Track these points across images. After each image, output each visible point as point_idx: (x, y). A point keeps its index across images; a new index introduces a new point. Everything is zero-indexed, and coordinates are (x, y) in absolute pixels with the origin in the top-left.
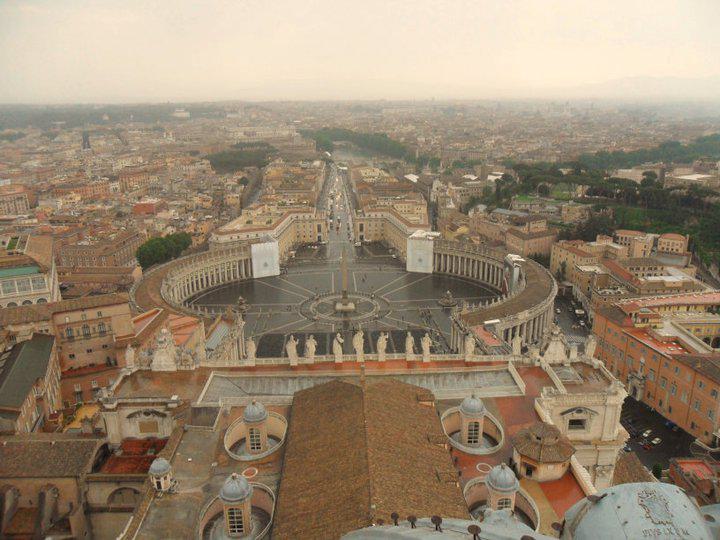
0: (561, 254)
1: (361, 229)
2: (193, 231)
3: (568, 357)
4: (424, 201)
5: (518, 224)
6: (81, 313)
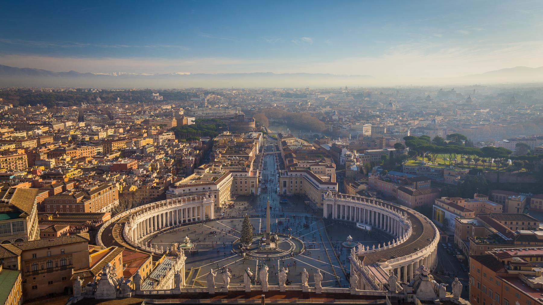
0: (442, 206)
1: (285, 185)
2: (155, 185)
3: (438, 296)
4: (334, 165)
5: (407, 184)
6: (47, 250)
